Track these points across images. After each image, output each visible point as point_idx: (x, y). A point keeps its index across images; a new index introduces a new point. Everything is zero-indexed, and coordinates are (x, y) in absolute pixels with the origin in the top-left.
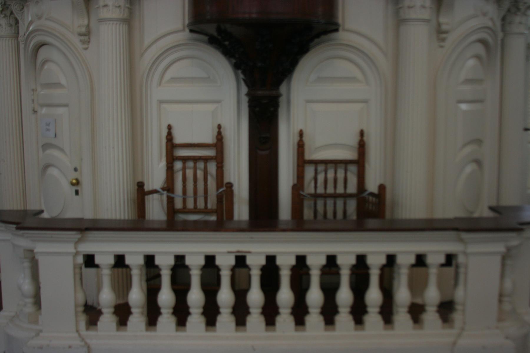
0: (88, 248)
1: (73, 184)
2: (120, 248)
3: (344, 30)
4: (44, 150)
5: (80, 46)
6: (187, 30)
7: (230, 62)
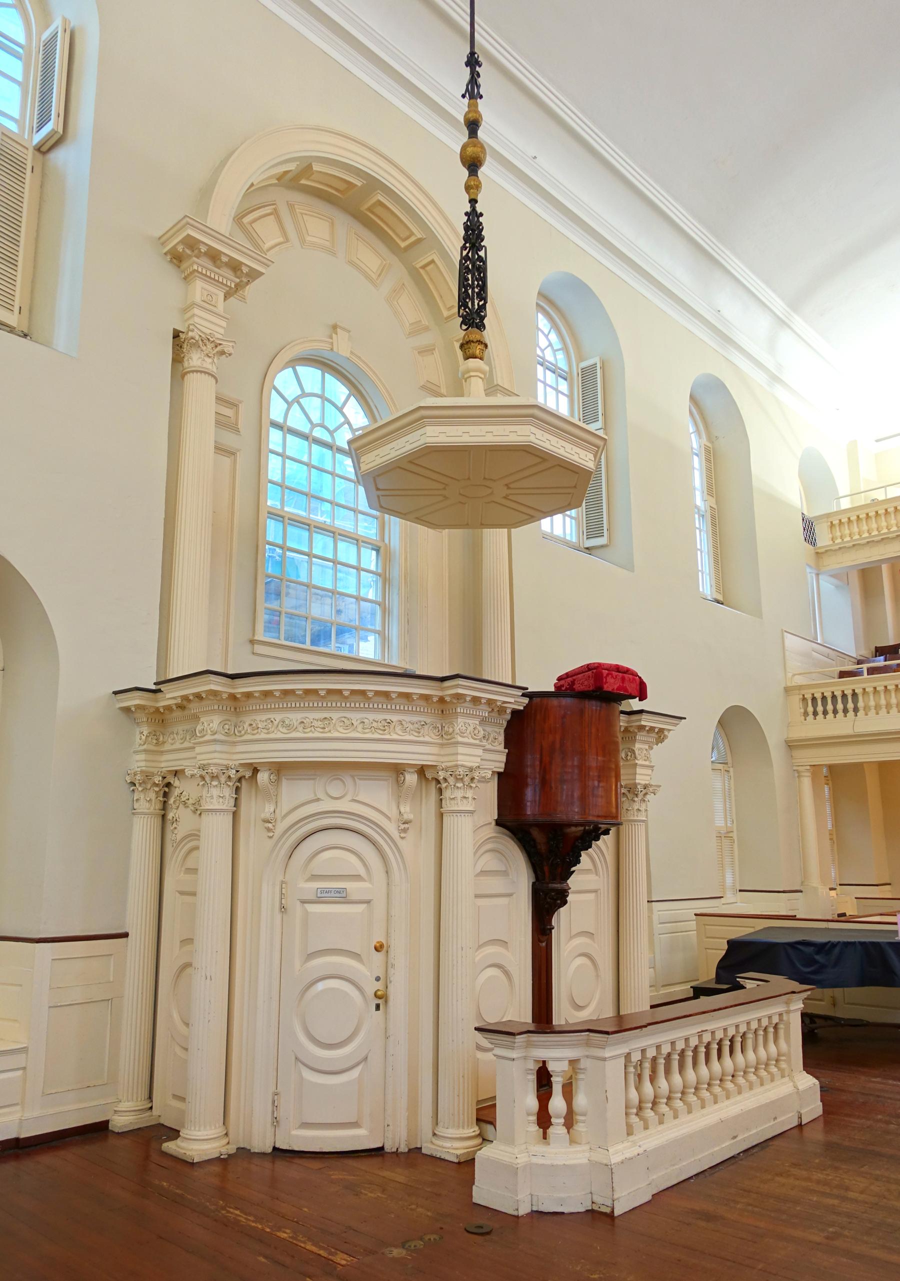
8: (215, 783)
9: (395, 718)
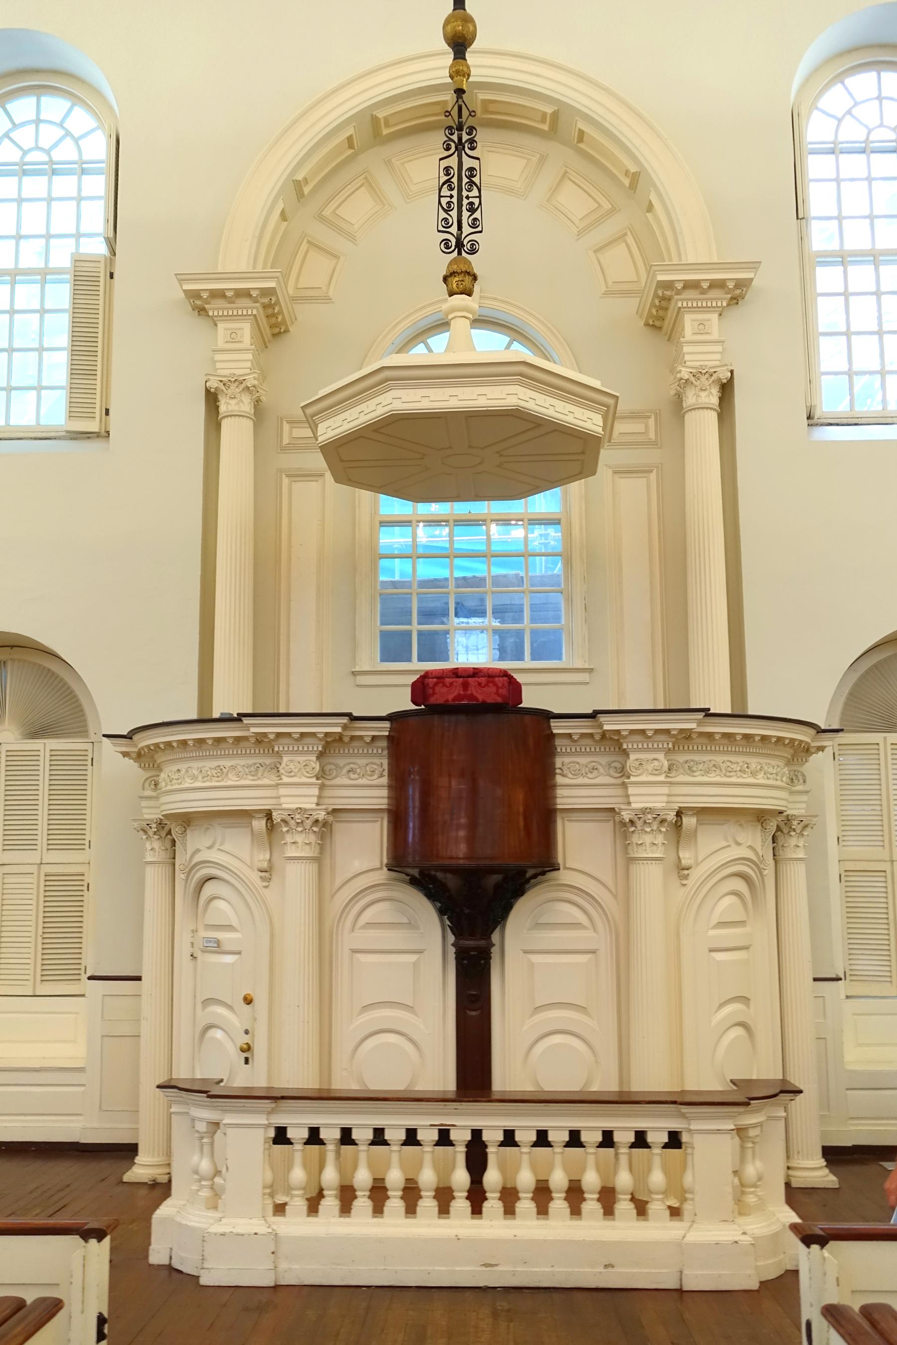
0: (281, 1120)
1: (243, 1050)
2: (314, 1121)
3: (566, 868)
4: (204, 1008)
5: (260, 884)
6: (385, 869)
7: (435, 907)
8: (300, 829)
9: (228, 763)
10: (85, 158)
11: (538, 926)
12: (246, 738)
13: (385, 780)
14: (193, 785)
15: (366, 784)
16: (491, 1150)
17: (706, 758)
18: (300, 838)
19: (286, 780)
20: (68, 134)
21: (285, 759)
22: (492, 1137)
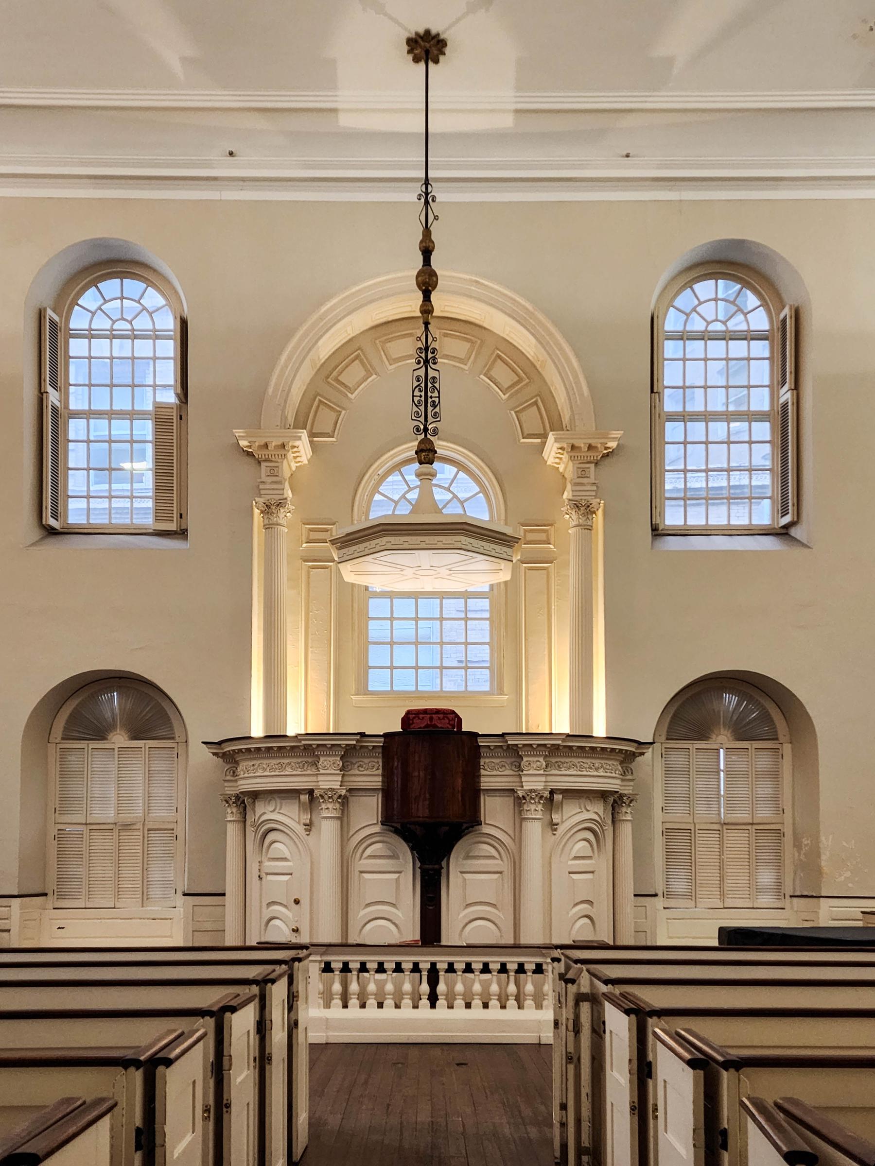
3: (486, 824)
5: (304, 833)
9: (286, 761)
10: (157, 328)
11: (468, 857)
12: (298, 747)
13: (380, 772)
14: (255, 776)
15: (370, 775)
16: (441, 973)
17: (568, 760)
18: (330, 806)
19: (322, 771)
20: (144, 309)
21: (322, 759)
22: (442, 966)
